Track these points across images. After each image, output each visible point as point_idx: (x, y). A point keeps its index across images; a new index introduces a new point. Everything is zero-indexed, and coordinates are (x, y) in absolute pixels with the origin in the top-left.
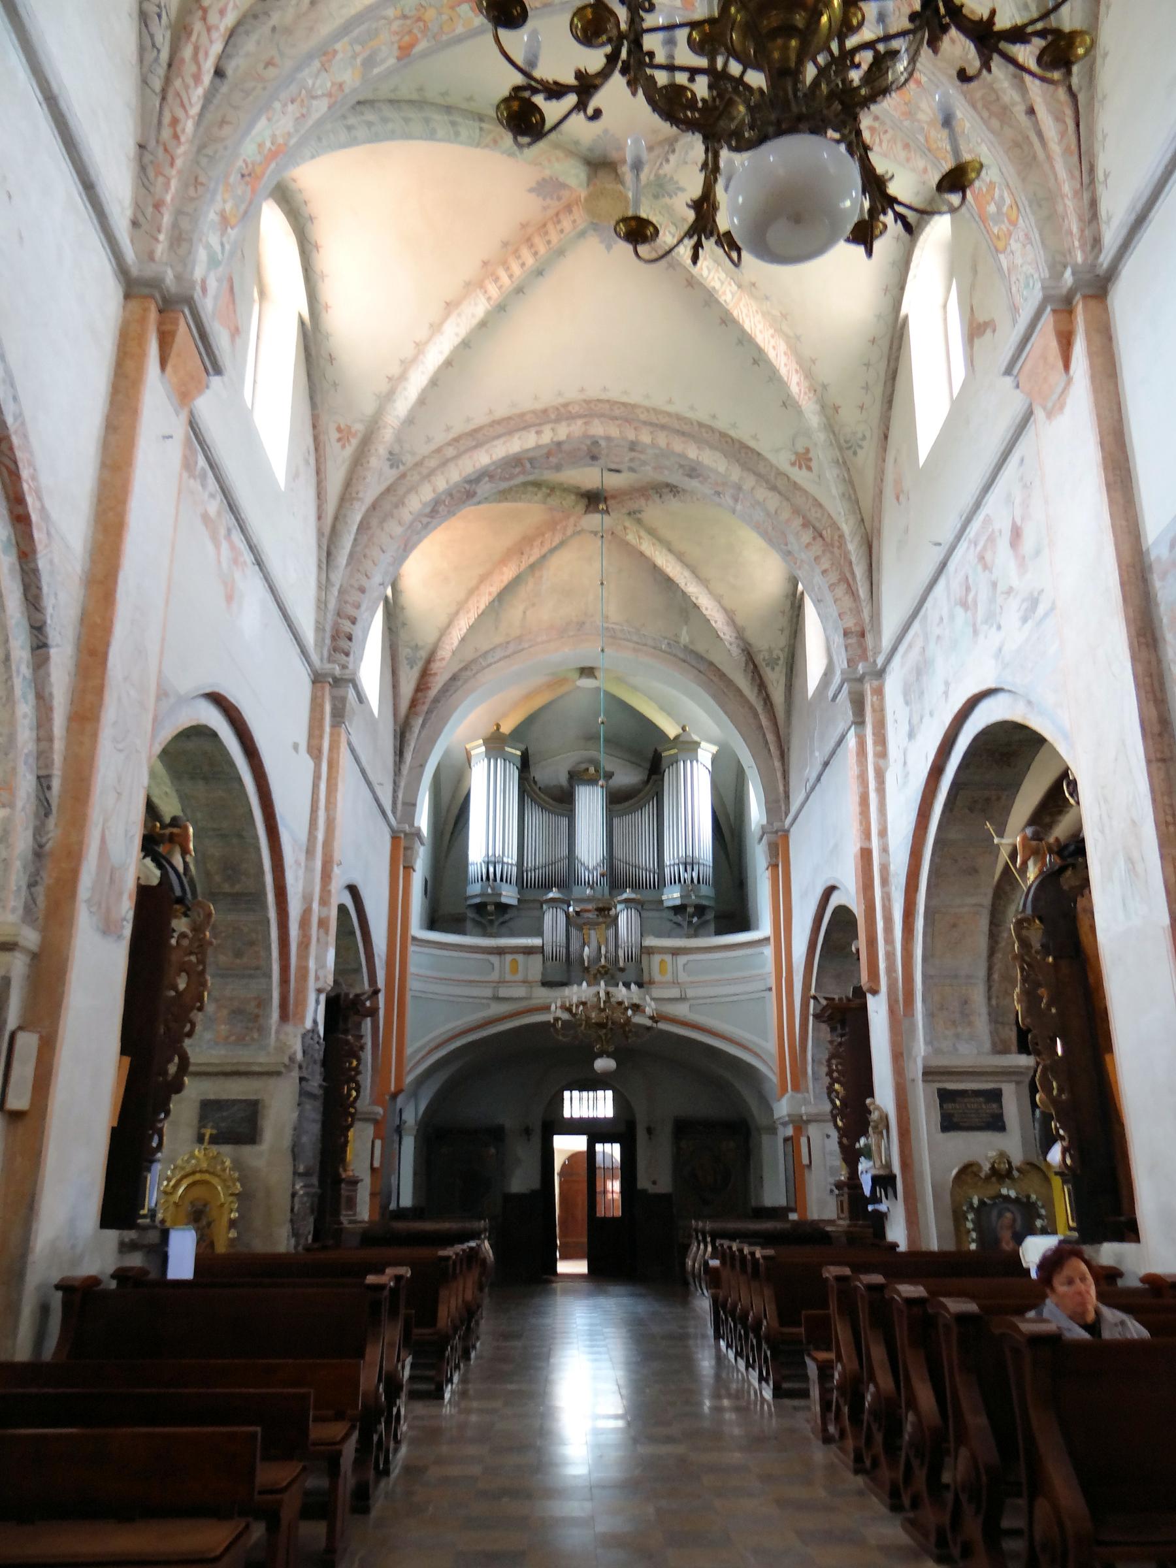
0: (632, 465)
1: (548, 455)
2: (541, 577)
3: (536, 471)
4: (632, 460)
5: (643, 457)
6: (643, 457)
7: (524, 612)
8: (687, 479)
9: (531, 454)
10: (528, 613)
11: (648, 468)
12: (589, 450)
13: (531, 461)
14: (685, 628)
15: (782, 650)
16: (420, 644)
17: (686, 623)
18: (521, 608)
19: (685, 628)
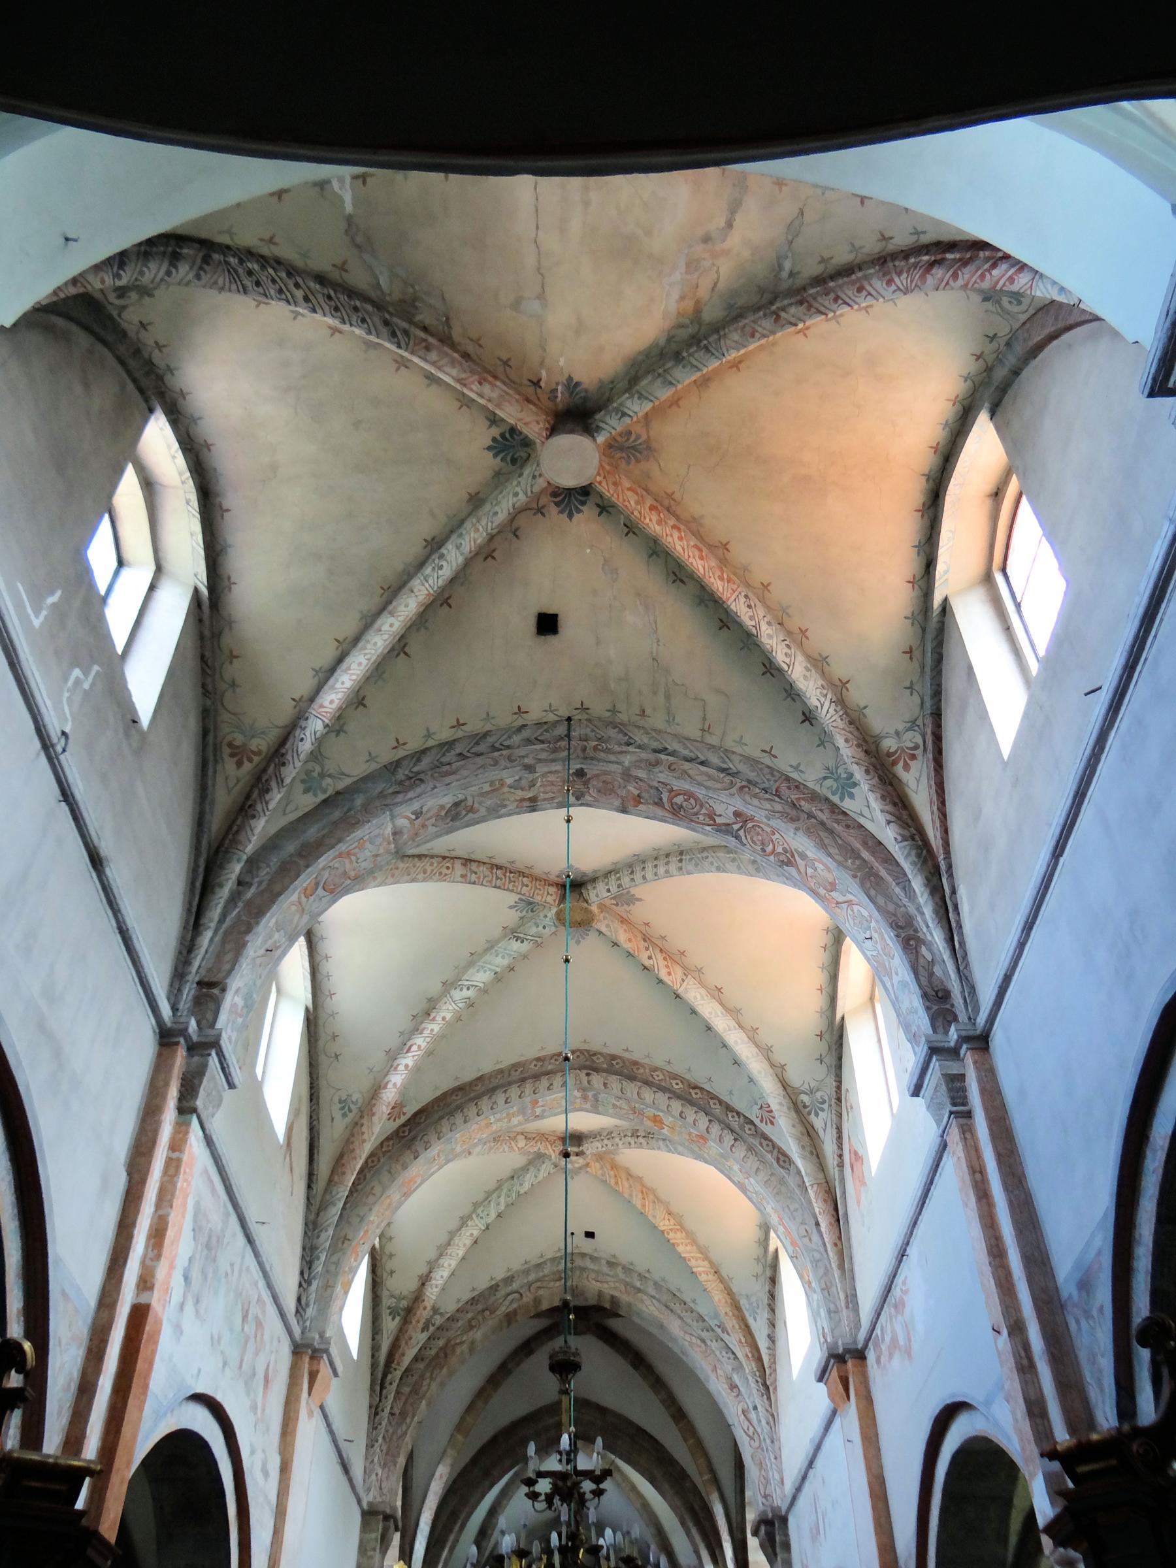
0: (531, 776)
1: (638, 800)
2: (682, 298)
3: (655, 784)
4: (532, 784)
5: (520, 794)
6: (520, 794)
7: (730, 225)
8: (461, 797)
9: (659, 812)
10: (722, 222)
11: (509, 781)
12: (586, 784)
13: (659, 803)
14: (349, 208)
15: (124, 308)
16: (977, 298)
17: (349, 219)
18: (734, 241)
19: (349, 208)
